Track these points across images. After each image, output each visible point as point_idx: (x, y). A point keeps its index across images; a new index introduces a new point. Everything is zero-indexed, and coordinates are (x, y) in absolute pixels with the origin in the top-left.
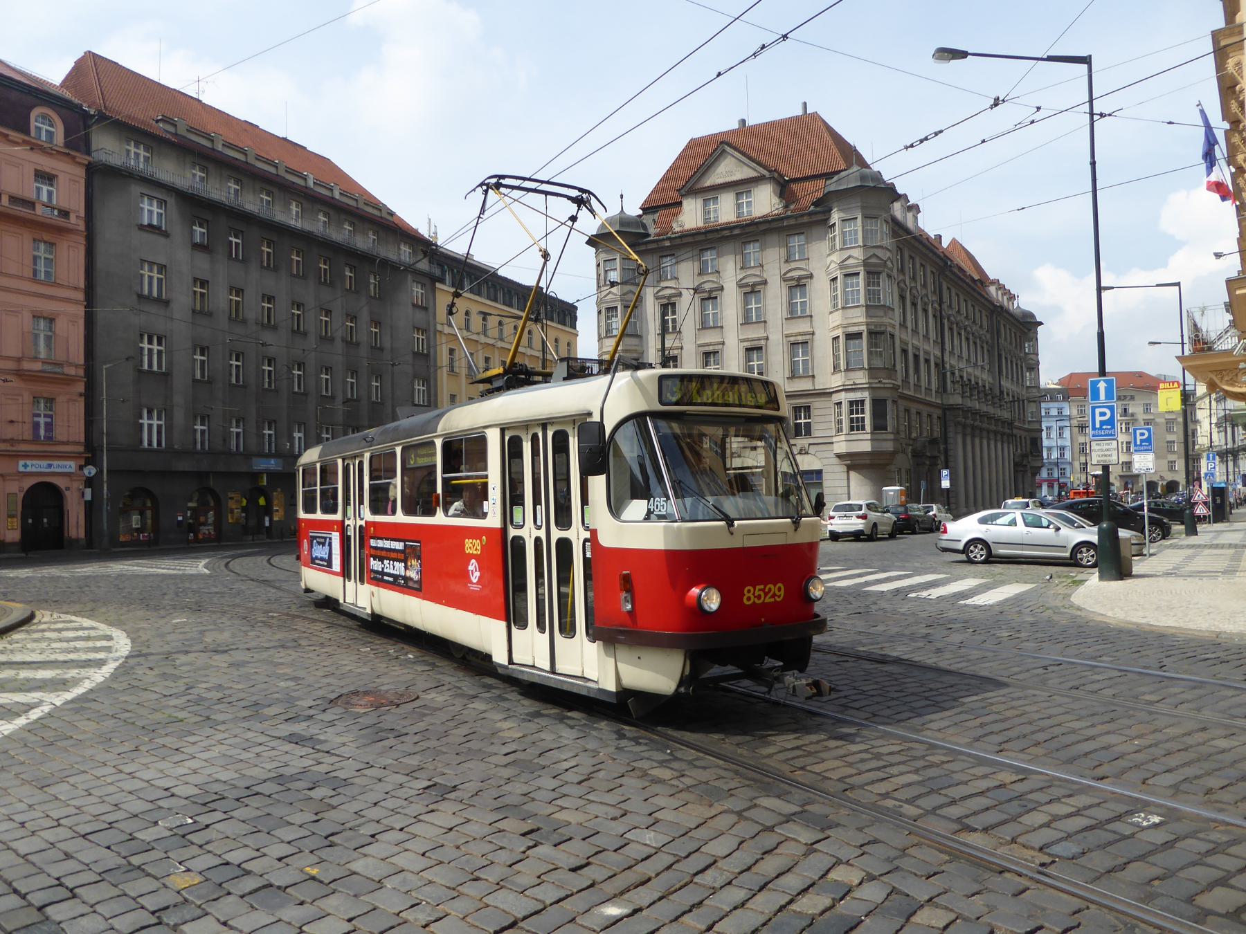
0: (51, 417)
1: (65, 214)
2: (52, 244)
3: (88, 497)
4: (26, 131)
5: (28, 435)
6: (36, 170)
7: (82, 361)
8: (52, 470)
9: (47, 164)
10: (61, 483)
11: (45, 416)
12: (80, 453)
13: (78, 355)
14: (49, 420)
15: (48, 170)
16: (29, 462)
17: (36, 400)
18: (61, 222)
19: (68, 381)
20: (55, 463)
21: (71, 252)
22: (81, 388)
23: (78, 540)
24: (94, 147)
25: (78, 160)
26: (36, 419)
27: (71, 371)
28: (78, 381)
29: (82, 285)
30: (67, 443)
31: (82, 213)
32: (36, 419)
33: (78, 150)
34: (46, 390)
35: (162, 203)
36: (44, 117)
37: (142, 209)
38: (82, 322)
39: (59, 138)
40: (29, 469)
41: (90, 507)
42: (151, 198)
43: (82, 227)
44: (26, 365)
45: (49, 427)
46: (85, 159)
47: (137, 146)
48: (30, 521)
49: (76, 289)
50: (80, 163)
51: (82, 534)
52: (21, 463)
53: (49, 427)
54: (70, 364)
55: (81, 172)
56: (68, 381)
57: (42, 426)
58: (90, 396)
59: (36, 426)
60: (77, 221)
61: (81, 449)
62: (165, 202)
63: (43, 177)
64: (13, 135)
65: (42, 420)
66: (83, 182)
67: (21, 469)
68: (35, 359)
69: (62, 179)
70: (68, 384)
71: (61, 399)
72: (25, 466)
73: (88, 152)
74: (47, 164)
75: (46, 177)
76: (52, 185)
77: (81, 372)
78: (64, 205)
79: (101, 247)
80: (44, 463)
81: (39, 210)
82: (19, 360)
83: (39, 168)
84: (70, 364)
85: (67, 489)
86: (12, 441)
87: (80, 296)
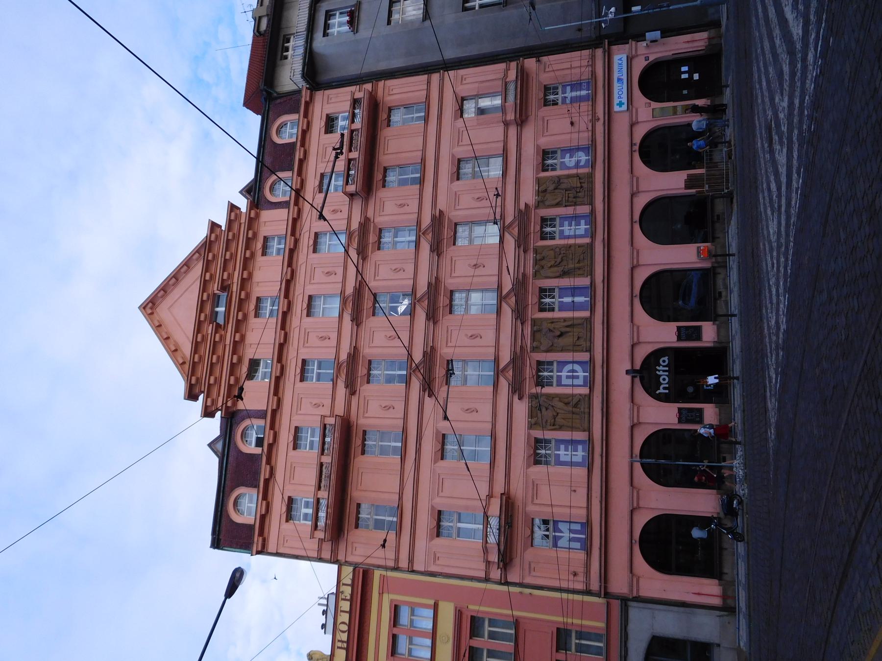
0: (564, 87)
1: (355, 102)
2: (390, 109)
3: (658, 34)
4: (292, 146)
5: (585, 106)
6: (326, 132)
7: (503, 66)
8: (625, 77)
9: (318, 124)
10: (639, 65)
11: (564, 92)
12: (604, 52)
13: (494, 71)
14: (568, 88)
15: (323, 124)
16: (616, 101)
17: (546, 103)
18: (365, 104)
19: (523, 77)
20: (616, 75)
21: (394, 92)
22: (530, 63)
23: (709, 39)
24: (294, 87)
25: (308, 99)
26: (568, 101)
27: (512, 75)
28: (522, 67)
29: (426, 76)
30: (593, 65)
31: (353, 88)
32: (568, 101)
33: (299, 101)
34: (535, 94)
35: (329, 15)
36: (278, 131)
37: (338, 32)
38: (462, 72)
39: (295, 117)
40: (625, 100)
41: (667, 33)
42: (327, 26)
43: (368, 86)
44: (511, 116)
45: (576, 86)
46: (305, 95)
47: (287, 49)
48: (685, 92)
49: (429, 82)
50: (312, 97)
51: (705, 35)
52: (616, 108)
53: (576, 86)
54: (506, 75)
55: (319, 95)
56: (523, 77)
57: (574, 94)
58: (538, 51)
59: (574, 100)
60: (360, 92)
61: (599, 52)
62: (327, 12)
63: (332, 126)
64: (298, 155)
65: (569, 94)
66: (327, 92)
67: (624, 107)
68: (503, 109)
69: (329, 109)
70: (527, 75)
71: (546, 78)
72: (620, 104)
73: (299, 92)
74: (318, 124)
75: (330, 124)
76: (337, 118)
77: (513, 64)
78: (347, 106)
79: (383, 66)
80: (616, 86)
81: (354, 127)
82: (506, 124)
83: (323, 130)
84: (506, 75)
85: (647, 59)
86: (594, 119)
87: (435, 77)
